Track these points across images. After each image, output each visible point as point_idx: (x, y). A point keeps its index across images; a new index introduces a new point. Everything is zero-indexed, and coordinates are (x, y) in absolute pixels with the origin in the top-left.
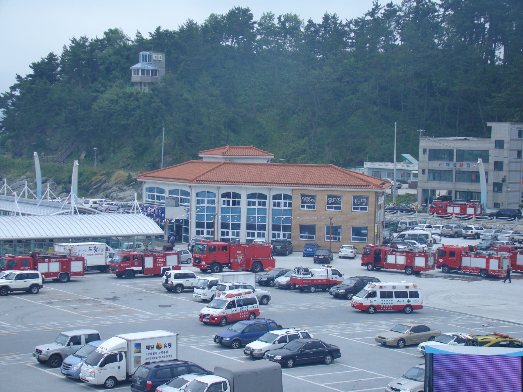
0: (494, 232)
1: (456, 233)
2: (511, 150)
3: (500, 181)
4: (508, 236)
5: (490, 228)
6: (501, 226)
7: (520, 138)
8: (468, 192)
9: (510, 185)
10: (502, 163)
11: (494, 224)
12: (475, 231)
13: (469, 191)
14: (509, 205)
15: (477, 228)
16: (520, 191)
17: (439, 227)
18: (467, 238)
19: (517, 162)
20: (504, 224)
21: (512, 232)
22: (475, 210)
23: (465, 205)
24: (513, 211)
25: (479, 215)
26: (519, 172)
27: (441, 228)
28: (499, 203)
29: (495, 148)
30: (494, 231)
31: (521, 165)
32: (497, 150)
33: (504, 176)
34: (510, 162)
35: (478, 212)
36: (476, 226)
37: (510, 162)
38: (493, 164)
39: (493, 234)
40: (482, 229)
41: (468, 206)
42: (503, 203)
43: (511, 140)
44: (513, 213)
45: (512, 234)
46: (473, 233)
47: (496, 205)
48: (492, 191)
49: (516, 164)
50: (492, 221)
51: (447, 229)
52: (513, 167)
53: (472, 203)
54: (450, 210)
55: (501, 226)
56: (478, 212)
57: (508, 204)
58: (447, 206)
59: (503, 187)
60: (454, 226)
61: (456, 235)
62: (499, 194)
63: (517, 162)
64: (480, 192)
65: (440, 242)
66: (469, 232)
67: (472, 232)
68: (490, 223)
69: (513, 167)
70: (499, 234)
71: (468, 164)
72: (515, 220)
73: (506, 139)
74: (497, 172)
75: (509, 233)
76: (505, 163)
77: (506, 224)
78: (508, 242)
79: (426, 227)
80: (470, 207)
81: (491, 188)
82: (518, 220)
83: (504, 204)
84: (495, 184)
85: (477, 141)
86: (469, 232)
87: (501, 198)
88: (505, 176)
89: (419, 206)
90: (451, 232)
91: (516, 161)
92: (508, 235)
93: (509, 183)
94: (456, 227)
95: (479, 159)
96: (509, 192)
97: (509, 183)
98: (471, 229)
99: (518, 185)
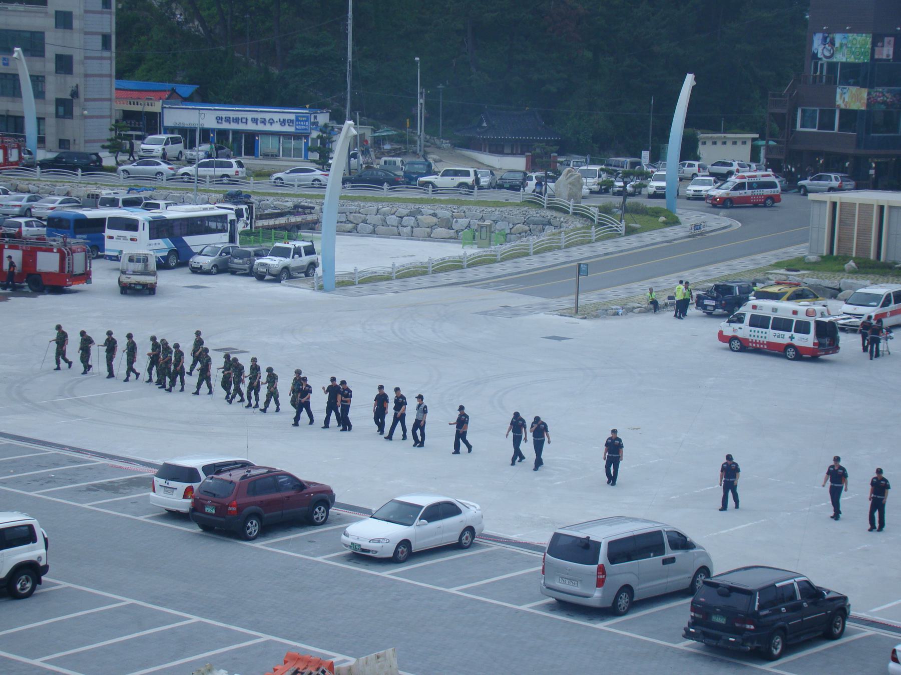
0: (25, 200)
2: (86, 33)
3: (67, 96)
4: (52, 209)
5: (27, 190)
7: (107, 8)
8: (8, 116)
9: (88, 103)
10: (70, 58)
11: (35, 182)
13: (11, 114)
14: (87, 145)
16: (110, 117)
19: (101, 58)
20: (54, 184)
21: (60, 199)
24: (87, 156)
25: (16, 163)
26: (108, 79)
28: (69, 141)
29: (56, 27)
31: (111, 64)
32: (60, 33)
33: (75, 85)
34: (86, 58)
35: (14, 156)
37: (86, 58)
38: (54, 61)
39: (24, 203)
42: (74, 140)
43: (86, 12)
45: (59, 204)
48: (55, 116)
49: (99, 61)
50: (72, 178)
52: (94, 67)
55: (47, 187)
57: (86, 142)
59: (74, 108)
62: (68, 121)
63: (101, 58)
64: (23, 117)
68: (27, 180)
69: (94, 67)
70: (34, 204)
71: (4, 59)
72: (77, 175)
73: (77, 12)
74: (61, 78)
75: (54, 202)
76: (77, 57)
77: (57, 184)
78: (32, 221)
81: (52, 109)
82: (82, 175)
83: (77, 142)
84: (59, 102)
85: (23, 11)
87: (73, 129)
88: (77, 86)
91: (98, 54)
92: (51, 205)
93: (86, 100)
95: (16, 49)
96: (86, 117)
97: (86, 100)
99: (107, 104)
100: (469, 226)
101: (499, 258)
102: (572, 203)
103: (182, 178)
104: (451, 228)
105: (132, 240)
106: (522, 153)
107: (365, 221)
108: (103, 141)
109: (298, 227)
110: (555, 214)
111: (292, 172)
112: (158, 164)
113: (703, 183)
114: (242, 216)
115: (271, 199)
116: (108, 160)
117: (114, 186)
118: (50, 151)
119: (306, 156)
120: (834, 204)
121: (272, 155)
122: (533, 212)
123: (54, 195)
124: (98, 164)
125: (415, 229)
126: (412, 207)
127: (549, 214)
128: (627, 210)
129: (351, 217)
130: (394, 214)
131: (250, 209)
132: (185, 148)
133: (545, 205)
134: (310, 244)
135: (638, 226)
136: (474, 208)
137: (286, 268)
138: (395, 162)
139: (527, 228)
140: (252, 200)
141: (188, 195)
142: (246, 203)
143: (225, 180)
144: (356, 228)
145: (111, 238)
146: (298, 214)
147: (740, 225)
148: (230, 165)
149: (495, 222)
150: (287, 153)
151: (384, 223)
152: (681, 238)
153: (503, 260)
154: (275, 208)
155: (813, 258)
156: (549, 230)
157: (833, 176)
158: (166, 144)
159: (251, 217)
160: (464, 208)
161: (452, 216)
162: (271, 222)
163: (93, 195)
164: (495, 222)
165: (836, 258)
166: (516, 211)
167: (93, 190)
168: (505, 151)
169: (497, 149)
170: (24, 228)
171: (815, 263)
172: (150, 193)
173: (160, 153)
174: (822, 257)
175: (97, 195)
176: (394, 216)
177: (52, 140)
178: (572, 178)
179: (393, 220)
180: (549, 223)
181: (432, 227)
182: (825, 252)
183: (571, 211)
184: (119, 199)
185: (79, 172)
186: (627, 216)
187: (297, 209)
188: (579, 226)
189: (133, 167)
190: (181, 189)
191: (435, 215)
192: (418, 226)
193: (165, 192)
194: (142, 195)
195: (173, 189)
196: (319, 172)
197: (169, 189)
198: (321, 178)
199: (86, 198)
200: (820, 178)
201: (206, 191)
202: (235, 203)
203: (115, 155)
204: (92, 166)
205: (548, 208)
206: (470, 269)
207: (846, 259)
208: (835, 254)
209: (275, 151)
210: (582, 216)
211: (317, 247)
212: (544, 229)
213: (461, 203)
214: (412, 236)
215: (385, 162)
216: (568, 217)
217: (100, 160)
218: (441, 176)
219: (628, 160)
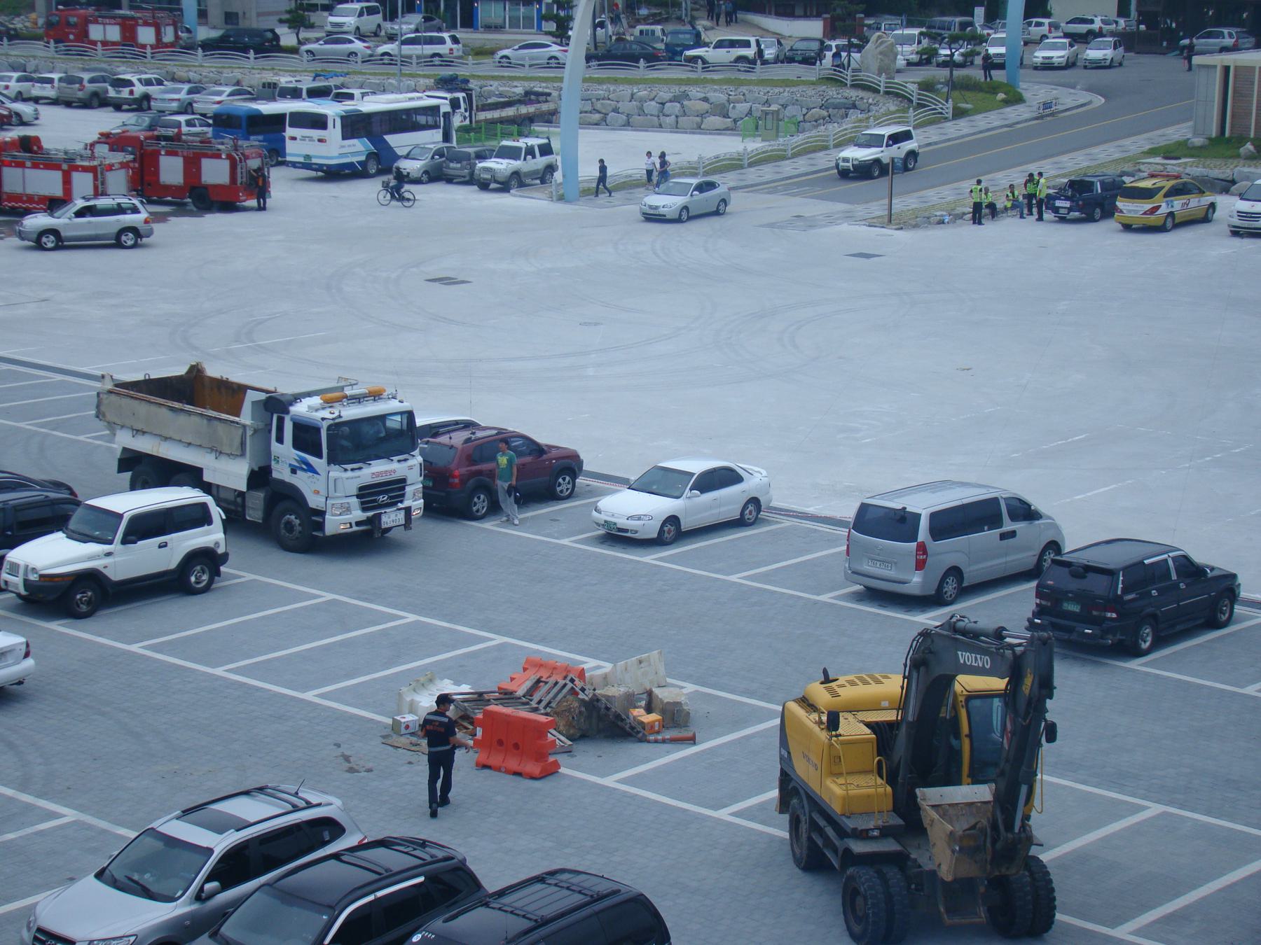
0: (185, 91)
1: (95, 94)
4: (219, 103)
5: (187, 79)
6: (211, 75)
11: (195, 69)
12: (139, 89)
14: (260, 19)
15: (148, 83)
17: (51, 81)
18: (125, 107)
21: (228, 90)
22: (158, 33)
23: (133, 18)
24: (259, 33)
25: (172, 45)
27: (56, 84)
28: (237, 14)
30: (186, 87)
35: (169, 36)
36: (144, 76)
39: (183, 95)
40: (160, 83)
41: (140, 21)
42: (244, 13)
44: (258, 39)
46: (137, 95)
47: (230, 17)
50: (244, 63)
51: (70, 86)
53: (148, 15)
54: (96, 32)
55: (211, 75)
56: (169, 36)
58: (86, 22)
60: (86, 76)
61: (95, 102)
65: (36, 122)
66: (125, 93)
67: (131, 92)
68: (187, 66)
72: (249, 58)
75: (219, 93)
77: (225, 71)
78: (194, 119)
79: (19, 80)
80: (146, 24)
82: (255, 58)
83: (247, 15)
86: (125, 93)
89: (41, 21)
90: (80, 94)
92: (218, 98)
94: (92, 81)
98: (129, 83)
100: (750, 113)
101: (790, 153)
102: (883, 78)
103: (381, 60)
104: (726, 116)
105: (320, 141)
106: (818, 15)
107: (616, 110)
108: (277, 13)
109: (531, 119)
110: (861, 93)
111: (521, 48)
112: (351, 42)
113: (1054, 47)
114: (459, 107)
115: (495, 84)
116: (287, 38)
117: (296, 71)
118: (214, 28)
119: (539, 27)
120: (1226, 69)
121: (496, 27)
122: (832, 92)
123: (221, 84)
124: (275, 43)
125: (680, 119)
126: (676, 90)
127: (853, 94)
128: (953, 85)
129: (598, 106)
130: (653, 99)
131: (470, 97)
132: (385, 19)
133: (849, 83)
134: (545, 141)
135: (969, 106)
136: (756, 89)
137: (516, 174)
138: (653, 32)
139: (825, 113)
140: (471, 86)
141: (390, 81)
142: (463, 90)
143: (437, 60)
144: (604, 119)
145: (294, 138)
146: (531, 102)
147: (1103, 100)
148: (441, 41)
149: (784, 106)
150: (515, 23)
151: (641, 111)
152: (1026, 121)
153: (795, 156)
154: (501, 95)
155: (1198, 141)
156: (854, 115)
157: (1226, 31)
158: (361, 15)
159: (470, 108)
160: (744, 89)
161: (728, 101)
162: (496, 114)
163: (269, 84)
164: (784, 106)
165: (1229, 140)
166: (810, 91)
167: (269, 77)
168: (796, 14)
169: (786, 11)
170: (185, 129)
171: (1201, 147)
172: (341, 79)
173: (352, 28)
174: (1210, 139)
175: (275, 84)
176: (653, 103)
177: (215, 14)
178: (884, 45)
179: (652, 107)
180: (854, 106)
181: (702, 115)
182: (1214, 135)
183: (882, 89)
184: (301, 89)
185: (252, 54)
186: (956, 94)
187: (530, 97)
188: (893, 108)
189: (319, 46)
190: (381, 74)
191: (705, 100)
192: (685, 114)
193: (360, 78)
194: (331, 82)
195: (370, 74)
196: (555, 48)
197: (365, 74)
198: (558, 54)
199: (261, 88)
200: (1209, 35)
201: (412, 76)
202: (450, 91)
203: (296, 31)
204: (267, 46)
205: (854, 86)
206: (752, 170)
207: (1242, 140)
208: (1227, 134)
209: (500, 21)
210: (897, 95)
211: (555, 145)
212: (847, 115)
213: (740, 83)
214: (676, 128)
215: (641, 32)
216: (878, 97)
217: (277, 38)
218: (714, 48)
219: (958, 19)
